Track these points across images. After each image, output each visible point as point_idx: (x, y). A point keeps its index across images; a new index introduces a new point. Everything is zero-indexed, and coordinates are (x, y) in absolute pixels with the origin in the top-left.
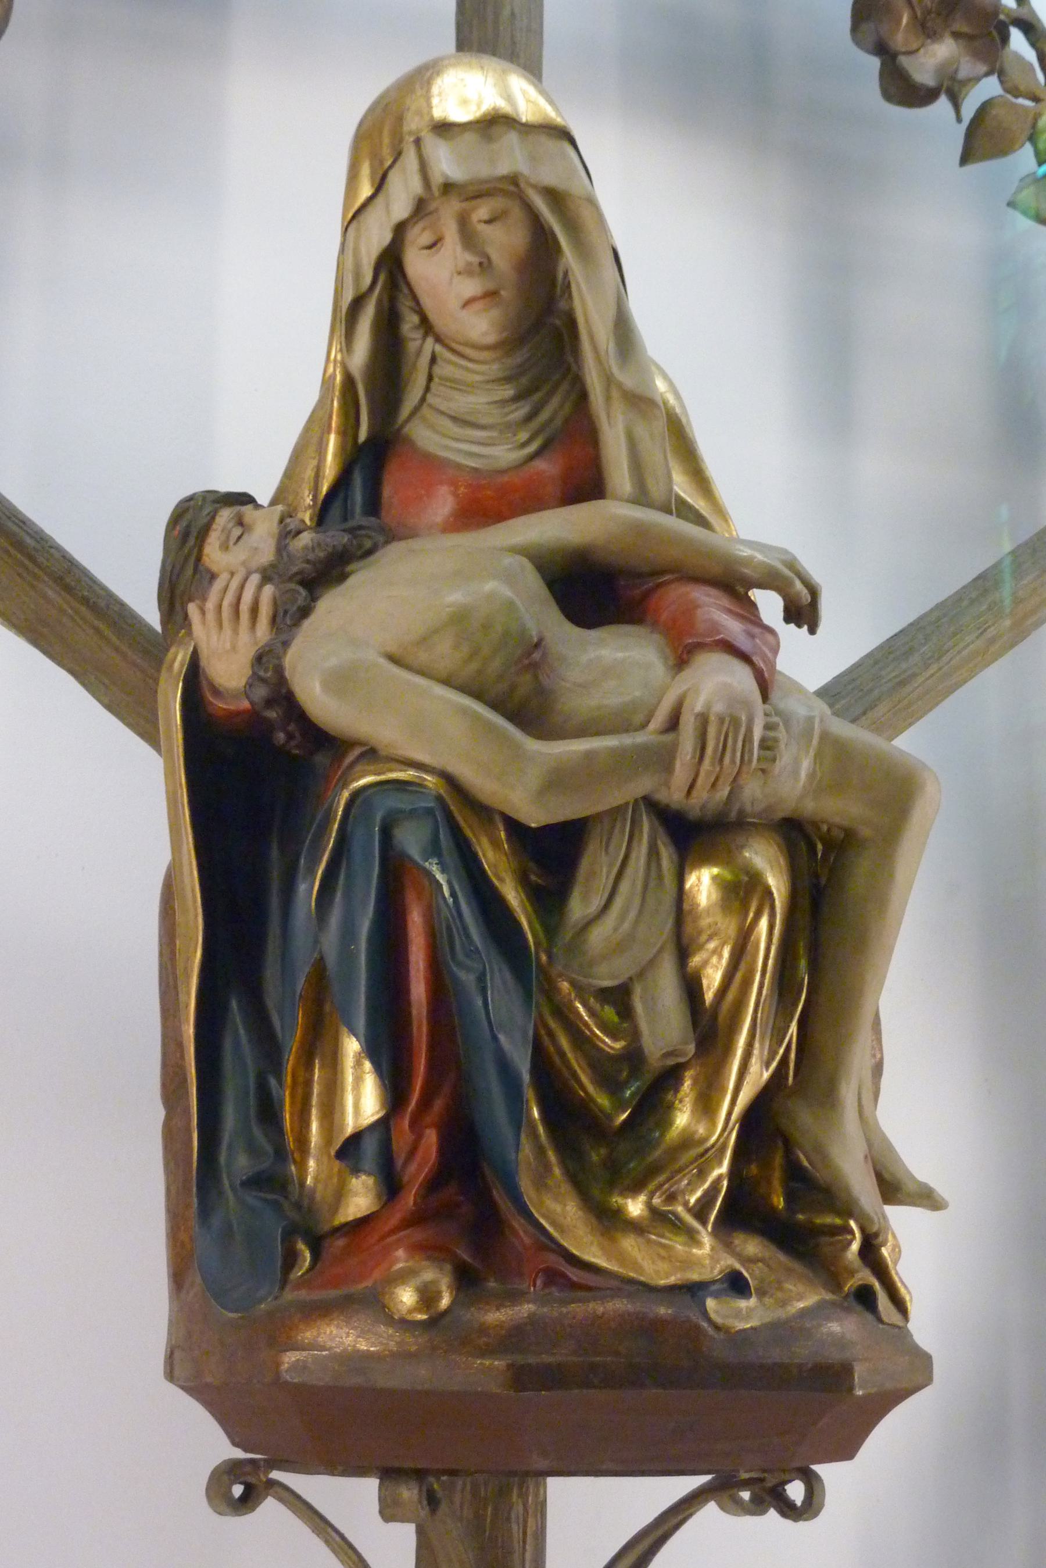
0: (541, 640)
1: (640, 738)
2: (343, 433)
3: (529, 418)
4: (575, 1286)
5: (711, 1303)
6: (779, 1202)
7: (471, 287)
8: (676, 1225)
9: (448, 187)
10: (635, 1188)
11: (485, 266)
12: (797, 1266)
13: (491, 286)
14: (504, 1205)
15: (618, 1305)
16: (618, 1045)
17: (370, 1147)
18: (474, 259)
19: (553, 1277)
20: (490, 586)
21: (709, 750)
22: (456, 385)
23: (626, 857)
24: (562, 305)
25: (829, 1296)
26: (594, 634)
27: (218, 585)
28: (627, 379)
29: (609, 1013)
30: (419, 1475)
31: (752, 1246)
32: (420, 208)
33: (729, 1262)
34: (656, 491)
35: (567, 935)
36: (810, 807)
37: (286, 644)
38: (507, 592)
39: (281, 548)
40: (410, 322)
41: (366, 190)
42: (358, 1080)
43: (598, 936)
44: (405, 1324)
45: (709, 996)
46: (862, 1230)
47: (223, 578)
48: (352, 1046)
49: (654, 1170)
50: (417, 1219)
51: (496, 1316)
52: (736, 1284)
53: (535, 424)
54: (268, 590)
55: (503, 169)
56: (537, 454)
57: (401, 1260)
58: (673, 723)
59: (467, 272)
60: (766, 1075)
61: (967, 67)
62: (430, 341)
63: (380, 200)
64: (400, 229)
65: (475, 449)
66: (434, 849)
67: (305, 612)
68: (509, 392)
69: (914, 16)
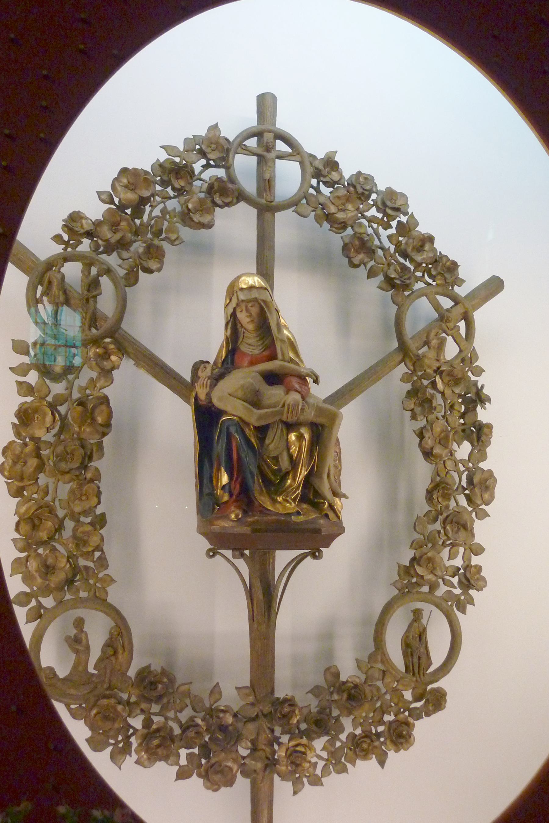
0: (258, 390)
1: (277, 409)
2: (226, 348)
3: (263, 343)
4: (266, 514)
5: (292, 517)
6: (312, 497)
7: (248, 320)
8: (288, 501)
9: (243, 301)
10: (279, 495)
11: (251, 315)
12: (314, 509)
13: (252, 319)
14: (253, 499)
15: (274, 517)
16: (276, 468)
17: (227, 487)
18: (248, 314)
19: (261, 512)
20: (248, 380)
21: (290, 411)
22: (248, 337)
23: (276, 432)
24: (268, 321)
25: (319, 515)
26: (271, 387)
27: (200, 380)
28: (279, 336)
29: (274, 462)
30: (238, 549)
31: (305, 506)
32: (238, 305)
33: (297, 509)
34: (287, 358)
35: (265, 447)
36: (315, 420)
37: (212, 392)
38: (252, 381)
39: (212, 372)
40: (239, 326)
41: (228, 301)
42: (225, 475)
43: (271, 447)
44: (233, 521)
45: (294, 459)
46: (328, 503)
47: (202, 378)
48: (223, 469)
49: (284, 491)
50: (236, 501)
51: (250, 519)
52: (298, 513)
53: (263, 345)
54: (209, 381)
55: (253, 296)
56: (264, 350)
57: (233, 508)
58: (283, 406)
59: (247, 317)
60: (306, 473)
61: (366, 260)
62: (243, 329)
63: (230, 303)
64: (235, 309)
65: (252, 350)
66: (237, 432)
67: (215, 385)
68: (258, 339)
69: (354, 249)
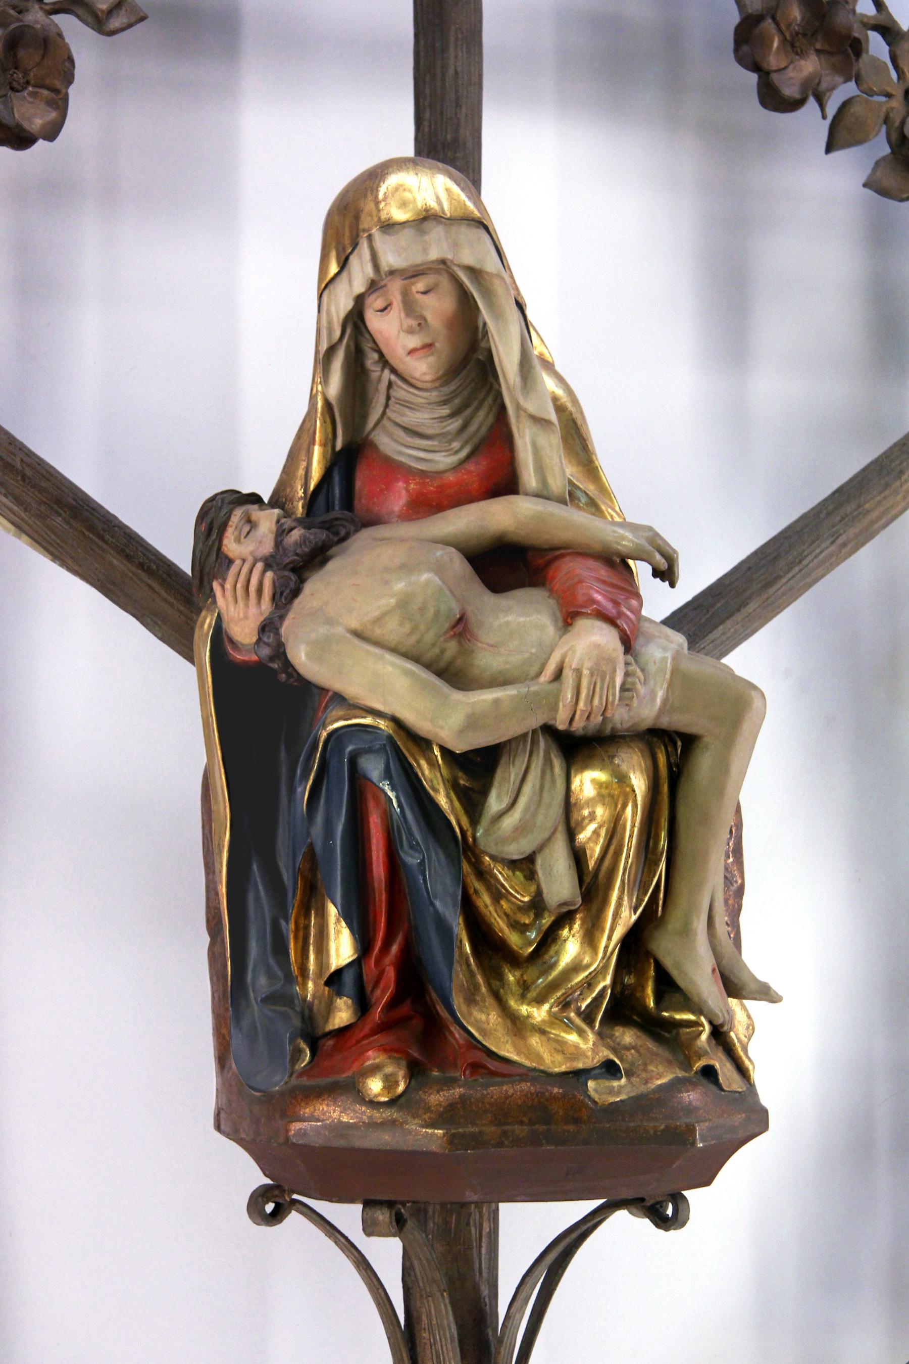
2: (324, 445)
5: (591, 1084)
9: (392, 273)
13: (428, 340)
17: (348, 979)
19: (476, 1067)
24: (483, 344)
25: (680, 1074)
27: (234, 569)
30: (390, 1204)
31: (627, 1036)
32: (373, 286)
33: (606, 1054)
37: (282, 618)
39: (278, 543)
40: (371, 358)
42: (338, 932)
44: (373, 1104)
45: (592, 864)
47: (238, 562)
48: (332, 911)
50: (384, 1027)
51: (437, 1098)
52: (610, 1069)
54: (269, 575)
55: (434, 254)
58: (558, 675)
59: (410, 331)
60: (634, 918)
62: (387, 372)
63: (344, 274)
64: (360, 300)
65: (422, 454)
67: (296, 593)
68: (445, 411)
69: (784, 40)
